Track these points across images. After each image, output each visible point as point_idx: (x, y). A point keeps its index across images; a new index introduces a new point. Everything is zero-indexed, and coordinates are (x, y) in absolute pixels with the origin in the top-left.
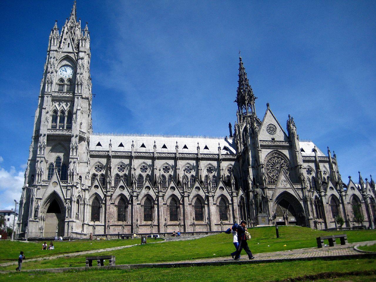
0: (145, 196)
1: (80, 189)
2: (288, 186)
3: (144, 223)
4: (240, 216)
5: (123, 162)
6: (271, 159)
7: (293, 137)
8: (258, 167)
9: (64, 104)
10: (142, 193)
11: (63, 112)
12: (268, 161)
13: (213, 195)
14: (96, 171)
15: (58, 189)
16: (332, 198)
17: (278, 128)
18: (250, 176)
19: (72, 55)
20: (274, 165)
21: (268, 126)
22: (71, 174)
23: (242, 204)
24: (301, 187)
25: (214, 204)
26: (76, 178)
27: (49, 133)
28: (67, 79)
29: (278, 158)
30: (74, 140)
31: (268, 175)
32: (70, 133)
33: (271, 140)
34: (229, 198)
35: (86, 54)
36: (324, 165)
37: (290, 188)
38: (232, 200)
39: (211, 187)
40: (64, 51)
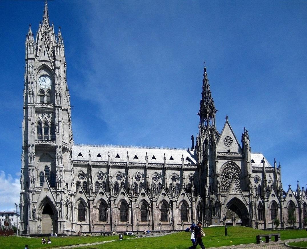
2: (238, 193)
6: (226, 169)
7: (246, 149)
8: (215, 176)
9: (46, 116)
11: (46, 123)
12: (223, 171)
13: (176, 200)
14: (80, 179)
16: (273, 204)
18: (207, 184)
20: (228, 174)
21: (226, 138)
22: (59, 181)
23: (199, 207)
24: (248, 194)
25: (177, 208)
26: (63, 185)
27: (36, 144)
29: (232, 168)
30: (59, 151)
31: (222, 183)
32: (55, 144)
34: (189, 203)
37: (239, 195)
38: (192, 205)
39: (175, 193)
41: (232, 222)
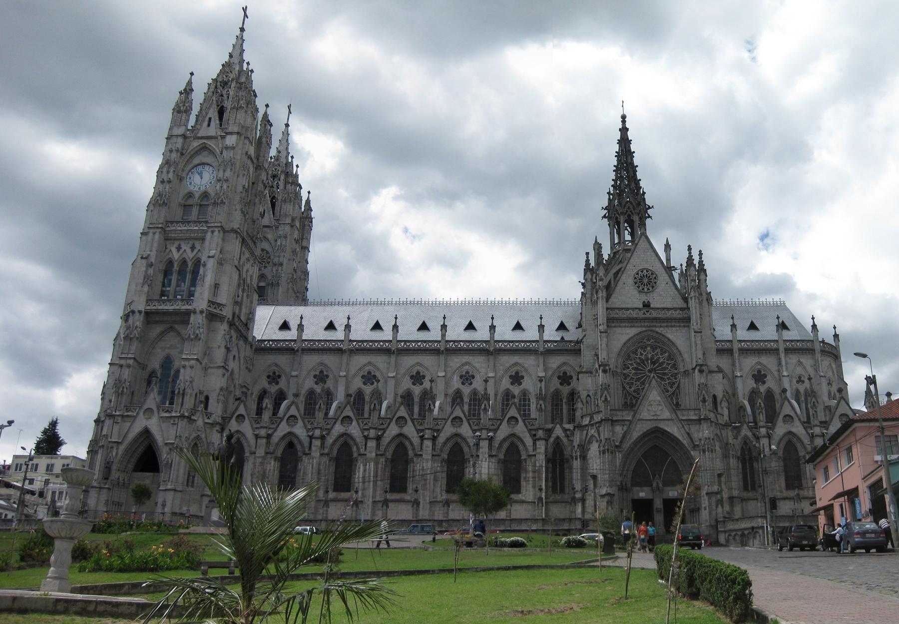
0: (342, 435)
1: (200, 423)
2: (666, 414)
3: (332, 495)
4: (550, 484)
5: (326, 362)
9: (186, 247)
10: (333, 431)
11: (184, 262)
15: (153, 424)
19: (211, 143)
27: (149, 308)
28: (200, 193)
29: (654, 348)
30: (197, 320)
31: (624, 388)
33: (641, 306)
35: (243, 137)
36: (799, 361)
38: (535, 449)
40: (199, 135)
41: (650, 497)
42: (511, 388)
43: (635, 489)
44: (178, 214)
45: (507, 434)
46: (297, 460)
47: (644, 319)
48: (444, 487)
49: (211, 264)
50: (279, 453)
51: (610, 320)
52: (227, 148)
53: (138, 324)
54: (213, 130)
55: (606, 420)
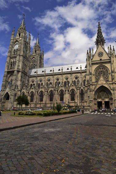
1: (16, 90)
2: (105, 82)
4: (80, 99)
9: (14, 59)
17: (104, 53)
29: (102, 69)
30: (15, 72)
38: (77, 92)
42: (75, 80)
43: (98, 99)
44: (13, 53)
45: (71, 89)
46: (33, 96)
47: (100, 63)
48: (60, 100)
49: (17, 61)
50: (30, 95)
51: (92, 64)
52: (20, 40)
53: (6, 74)
54: (18, 37)
55: (91, 85)
